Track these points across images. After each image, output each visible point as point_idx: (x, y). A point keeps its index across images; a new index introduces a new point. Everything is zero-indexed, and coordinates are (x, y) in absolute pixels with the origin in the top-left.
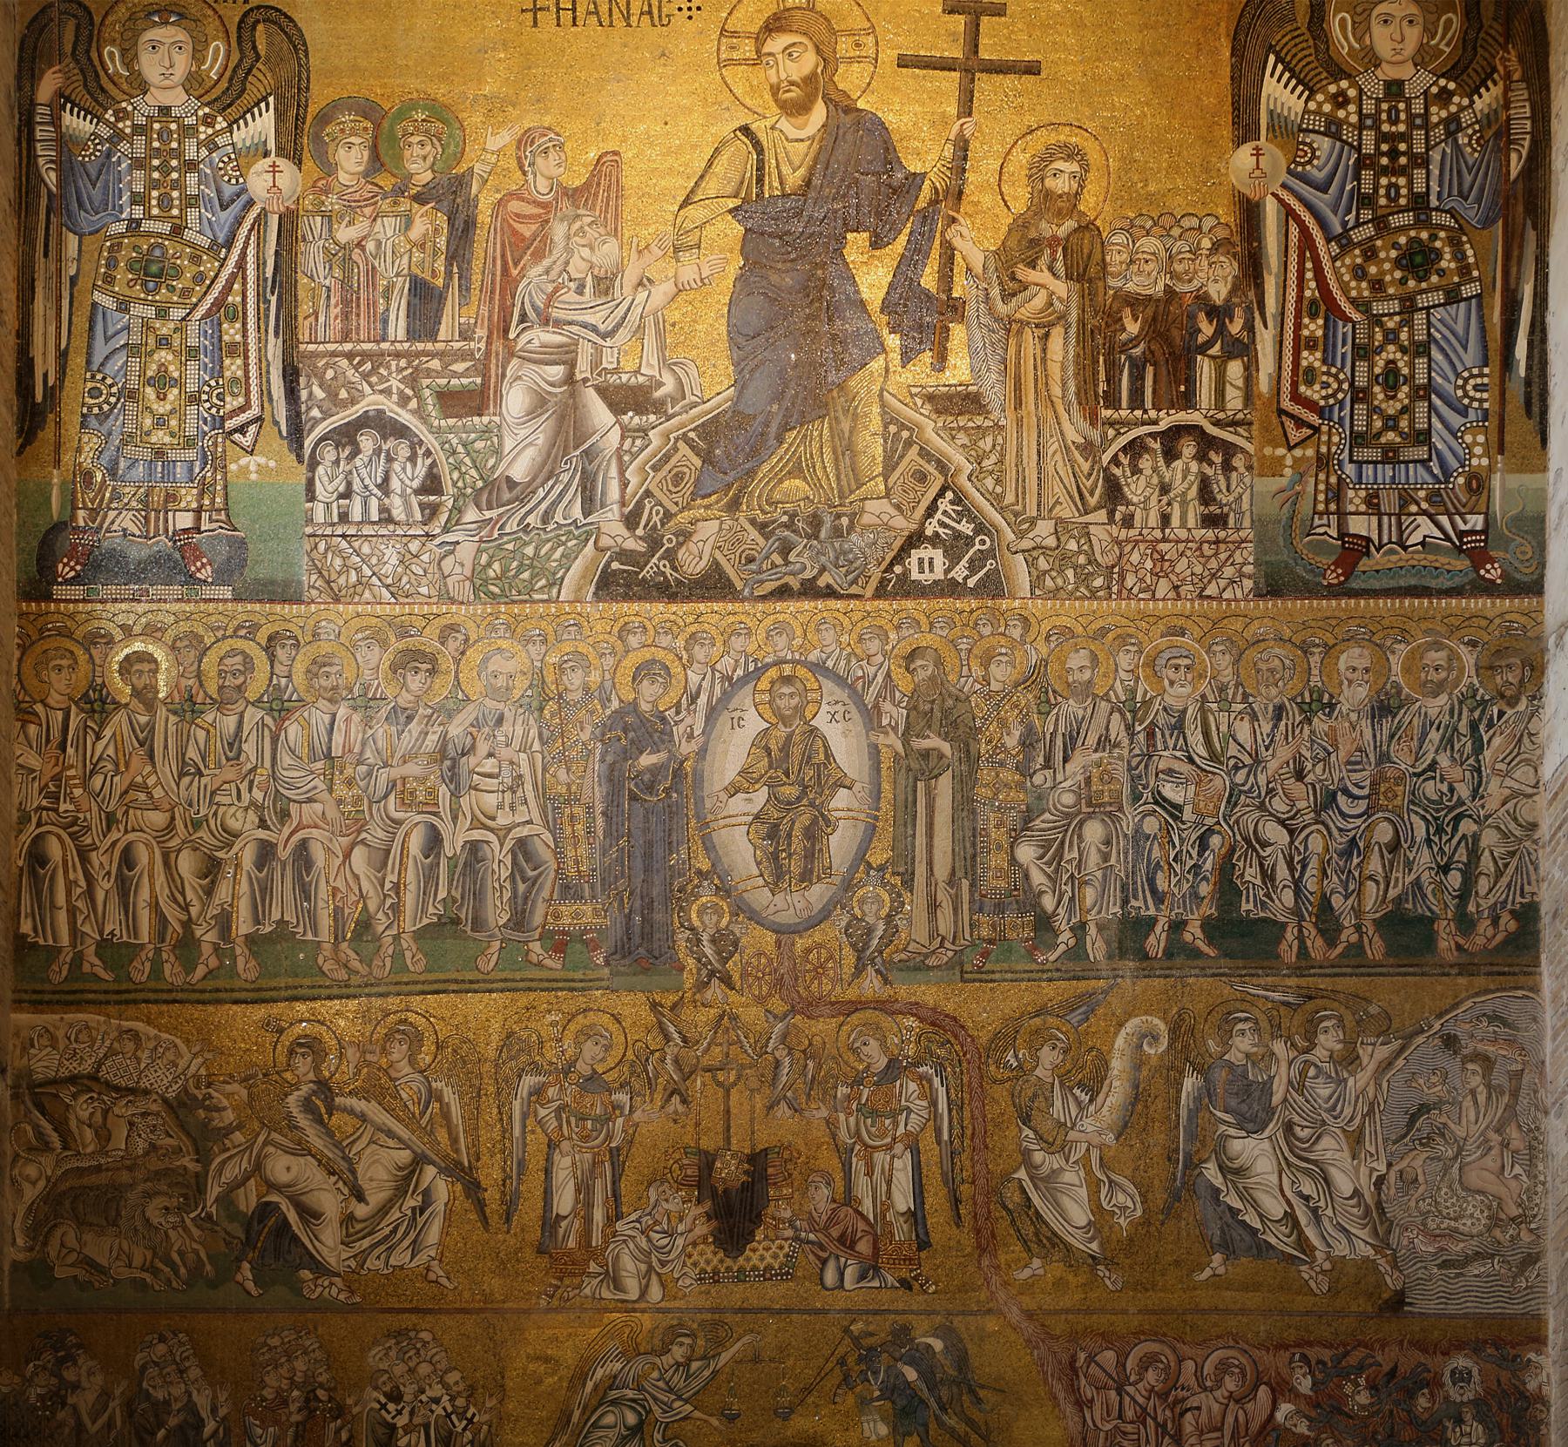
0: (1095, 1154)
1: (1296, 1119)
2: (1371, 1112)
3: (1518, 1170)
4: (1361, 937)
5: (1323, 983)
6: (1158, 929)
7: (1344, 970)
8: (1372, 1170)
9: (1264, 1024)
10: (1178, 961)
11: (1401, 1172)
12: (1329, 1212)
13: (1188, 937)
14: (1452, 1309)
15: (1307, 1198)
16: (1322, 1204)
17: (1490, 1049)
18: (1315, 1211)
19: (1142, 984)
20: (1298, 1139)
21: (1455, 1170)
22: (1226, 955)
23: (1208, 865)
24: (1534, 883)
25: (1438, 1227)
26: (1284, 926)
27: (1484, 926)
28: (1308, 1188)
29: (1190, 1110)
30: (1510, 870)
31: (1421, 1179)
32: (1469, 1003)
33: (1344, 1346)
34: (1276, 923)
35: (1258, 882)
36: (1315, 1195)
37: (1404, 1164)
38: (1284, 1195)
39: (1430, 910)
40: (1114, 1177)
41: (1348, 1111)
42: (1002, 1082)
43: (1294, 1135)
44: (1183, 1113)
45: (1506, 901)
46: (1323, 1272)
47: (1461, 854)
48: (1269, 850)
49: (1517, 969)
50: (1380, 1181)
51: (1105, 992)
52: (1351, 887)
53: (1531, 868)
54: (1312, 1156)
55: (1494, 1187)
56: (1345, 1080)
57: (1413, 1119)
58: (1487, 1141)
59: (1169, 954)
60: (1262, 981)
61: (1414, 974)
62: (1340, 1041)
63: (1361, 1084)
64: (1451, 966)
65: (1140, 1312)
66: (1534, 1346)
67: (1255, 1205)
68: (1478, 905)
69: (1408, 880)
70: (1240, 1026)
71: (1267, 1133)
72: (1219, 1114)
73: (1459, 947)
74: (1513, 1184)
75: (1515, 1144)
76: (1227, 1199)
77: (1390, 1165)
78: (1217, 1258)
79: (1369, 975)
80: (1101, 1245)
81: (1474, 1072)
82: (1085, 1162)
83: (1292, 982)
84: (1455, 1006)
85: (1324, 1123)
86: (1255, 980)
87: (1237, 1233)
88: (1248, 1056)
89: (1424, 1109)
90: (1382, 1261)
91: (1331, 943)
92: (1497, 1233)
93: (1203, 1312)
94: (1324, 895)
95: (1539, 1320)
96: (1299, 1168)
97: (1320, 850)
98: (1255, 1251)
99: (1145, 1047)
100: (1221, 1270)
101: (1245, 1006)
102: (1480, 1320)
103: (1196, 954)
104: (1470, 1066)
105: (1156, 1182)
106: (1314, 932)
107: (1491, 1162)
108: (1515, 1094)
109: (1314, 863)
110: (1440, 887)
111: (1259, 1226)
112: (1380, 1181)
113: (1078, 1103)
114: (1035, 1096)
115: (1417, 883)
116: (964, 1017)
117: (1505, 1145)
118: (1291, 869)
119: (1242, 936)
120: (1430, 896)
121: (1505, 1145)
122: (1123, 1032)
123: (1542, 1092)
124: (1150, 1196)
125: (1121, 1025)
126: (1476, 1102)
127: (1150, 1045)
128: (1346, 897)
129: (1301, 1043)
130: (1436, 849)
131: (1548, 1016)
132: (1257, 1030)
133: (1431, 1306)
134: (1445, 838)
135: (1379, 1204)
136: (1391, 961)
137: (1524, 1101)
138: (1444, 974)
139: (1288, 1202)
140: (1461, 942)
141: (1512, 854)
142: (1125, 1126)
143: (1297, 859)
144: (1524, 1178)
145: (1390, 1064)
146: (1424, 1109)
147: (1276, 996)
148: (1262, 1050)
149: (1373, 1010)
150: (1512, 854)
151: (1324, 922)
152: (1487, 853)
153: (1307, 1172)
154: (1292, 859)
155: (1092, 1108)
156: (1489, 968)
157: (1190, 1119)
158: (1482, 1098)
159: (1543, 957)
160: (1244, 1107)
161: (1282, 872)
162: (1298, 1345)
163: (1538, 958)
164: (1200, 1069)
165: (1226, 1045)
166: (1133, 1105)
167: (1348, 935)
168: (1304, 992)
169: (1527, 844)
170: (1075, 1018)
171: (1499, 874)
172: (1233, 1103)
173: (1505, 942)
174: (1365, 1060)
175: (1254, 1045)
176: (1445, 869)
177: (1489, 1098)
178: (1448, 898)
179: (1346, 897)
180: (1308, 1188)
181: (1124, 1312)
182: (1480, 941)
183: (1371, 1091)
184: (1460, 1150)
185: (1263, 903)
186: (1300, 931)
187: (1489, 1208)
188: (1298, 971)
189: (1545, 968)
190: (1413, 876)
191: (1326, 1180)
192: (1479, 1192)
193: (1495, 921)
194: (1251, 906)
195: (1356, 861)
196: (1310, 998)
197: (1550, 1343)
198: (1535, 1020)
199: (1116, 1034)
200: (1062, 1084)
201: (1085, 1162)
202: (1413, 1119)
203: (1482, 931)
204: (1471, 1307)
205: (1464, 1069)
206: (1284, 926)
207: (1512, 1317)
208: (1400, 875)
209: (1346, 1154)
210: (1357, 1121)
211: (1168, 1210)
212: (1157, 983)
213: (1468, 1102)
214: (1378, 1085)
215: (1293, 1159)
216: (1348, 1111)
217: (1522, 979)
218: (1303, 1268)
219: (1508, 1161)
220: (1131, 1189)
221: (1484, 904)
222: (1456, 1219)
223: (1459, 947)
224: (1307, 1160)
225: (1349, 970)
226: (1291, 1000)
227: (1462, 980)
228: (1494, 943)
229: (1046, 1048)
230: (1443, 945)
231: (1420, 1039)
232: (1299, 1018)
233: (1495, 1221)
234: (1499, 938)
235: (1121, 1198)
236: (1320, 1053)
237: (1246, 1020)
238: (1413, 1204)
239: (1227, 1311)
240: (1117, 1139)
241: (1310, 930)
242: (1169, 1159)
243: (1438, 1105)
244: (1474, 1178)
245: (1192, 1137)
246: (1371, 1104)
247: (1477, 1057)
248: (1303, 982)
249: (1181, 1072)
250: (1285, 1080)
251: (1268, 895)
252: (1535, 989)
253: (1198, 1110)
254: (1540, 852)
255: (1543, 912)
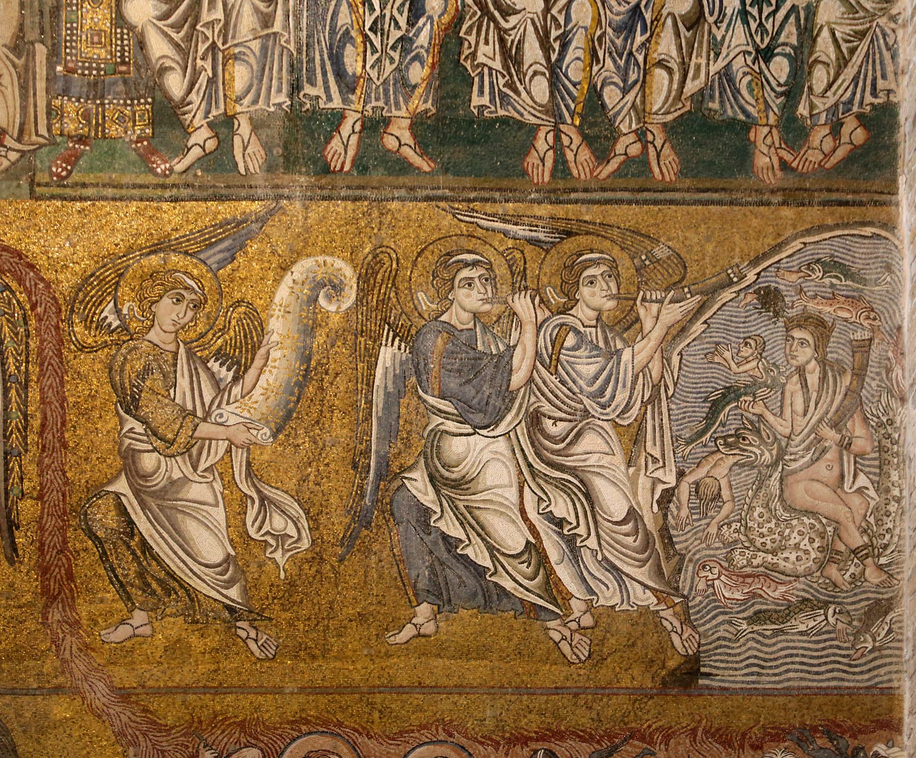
0: (239, 458)
1: (547, 408)
2: (654, 399)
3: (862, 480)
4: (645, 148)
5: (589, 214)
6: (346, 129)
7: (619, 195)
8: (656, 481)
9: (501, 270)
10: (377, 176)
11: (697, 484)
12: (592, 542)
13: (390, 143)
14: (767, 682)
15: (560, 523)
16: (582, 530)
17: (827, 310)
18: (571, 541)
19: (319, 209)
20: (548, 437)
21: (774, 482)
22: (446, 171)
23: (423, 39)
24: (891, 76)
25: (749, 564)
26: (534, 129)
27: (820, 136)
28: (561, 507)
29: (387, 395)
30: (858, 58)
31: (725, 494)
32: (797, 245)
33: (610, 738)
34: (521, 125)
35: (497, 65)
36: (572, 519)
37: (701, 473)
38: (525, 518)
39: (744, 111)
40: (268, 491)
41: (622, 397)
42: (92, 349)
43: (543, 431)
44: (378, 398)
45: (851, 102)
46: (581, 629)
47: (790, 35)
48: (513, 20)
49: (864, 198)
50: (667, 497)
51: (262, 220)
52: (633, 77)
53: (887, 55)
54: (569, 462)
55: (828, 505)
56: (618, 353)
57: (715, 408)
58: (819, 440)
59: (361, 165)
60: (499, 209)
61: (720, 203)
62: (611, 297)
63: (641, 358)
64: (773, 192)
65: (302, 690)
66: (885, 733)
67: (483, 533)
68: (812, 106)
69: (713, 69)
70: (465, 273)
71: (502, 428)
72: (431, 400)
73: (784, 165)
74: (856, 501)
75: (860, 444)
76: (442, 525)
77: (681, 475)
78: (424, 610)
79: (656, 202)
80: (245, 591)
81: (803, 342)
82: (223, 470)
83: (543, 210)
84: (777, 248)
85: (586, 413)
86: (489, 208)
87: (454, 574)
88: (476, 316)
89: (731, 394)
90: (667, 614)
91: (602, 155)
92: (833, 571)
93: (400, 690)
94: (592, 87)
95: (890, 694)
96: (547, 479)
97: (588, 22)
98: (480, 599)
99: (322, 301)
100: (429, 628)
101: (472, 244)
102: (805, 696)
103: (403, 167)
104: (797, 334)
105: (334, 500)
106: (577, 140)
107: (825, 470)
108: (860, 374)
109: (578, 41)
110: (760, 80)
111: (488, 563)
112: (667, 497)
113: (216, 382)
114: (147, 370)
115: (726, 74)
116: (33, 248)
117: (845, 445)
118: (546, 46)
119: (473, 143)
120: (744, 92)
121: (845, 445)
122: (288, 279)
123: (898, 371)
124: (323, 519)
125: (284, 268)
126: (804, 385)
127: (329, 298)
128: (625, 91)
129: (556, 299)
130: (754, 26)
131: (906, 263)
132: (490, 279)
133: (737, 678)
134: (766, 10)
135: (664, 531)
136: (688, 183)
137: (872, 384)
138: (762, 203)
139: (532, 529)
140: (788, 157)
141: (861, 35)
142: (288, 416)
143: (554, 34)
144: (872, 492)
145: (683, 330)
146: (731, 394)
147: (521, 231)
148: (497, 309)
149: (660, 252)
150: (861, 35)
151: (592, 125)
152: (825, 33)
153: (562, 486)
154: (547, 33)
155: (236, 390)
156: (825, 196)
157: (387, 406)
158: (813, 379)
159: (901, 180)
160: (470, 391)
161: (532, 52)
162: (541, 738)
163: (894, 181)
164: (404, 335)
165: (445, 298)
166: (301, 386)
167: (627, 145)
168: (562, 225)
169: (882, 21)
170: (214, 256)
171: (843, 62)
172: (453, 384)
173: (849, 160)
174: (648, 324)
175: (485, 301)
176: (767, 54)
177: (823, 378)
178: (769, 95)
179: (625, 91)
180: (561, 507)
181: (278, 690)
182: (814, 157)
183: (655, 368)
184: (782, 453)
185: (503, 96)
186: (557, 138)
187: (822, 535)
188: (552, 195)
189: (904, 195)
190: (721, 64)
191: (588, 496)
192: (808, 513)
193: (836, 129)
194: (485, 100)
195: (639, 39)
196: (569, 234)
197: (906, 730)
198: (888, 268)
199: (277, 281)
200: (190, 354)
201: (223, 470)
202: (715, 408)
203: (816, 143)
204: (794, 679)
205: (788, 338)
206: (534, 129)
207: (852, 692)
208: (703, 61)
209: (619, 459)
210: (635, 411)
211: (350, 541)
212: (342, 208)
213: (793, 385)
214: (666, 360)
215: (539, 466)
216: (622, 397)
217: (871, 212)
218: (551, 624)
219: (849, 469)
220: (295, 509)
221: (821, 105)
222: (774, 552)
223: (784, 165)
224: (561, 468)
225: (626, 195)
226: (541, 236)
227: (788, 212)
228: (834, 160)
229: (166, 301)
230: (762, 161)
231: (727, 295)
232: (553, 261)
233: (829, 555)
234: (841, 153)
235: (278, 522)
236: (583, 313)
237: (475, 264)
238: (713, 530)
239: (436, 689)
240: (275, 435)
241: (572, 136)
242: (355, 466)
243: (751, 388)
244: (800, 493)
245: (390, 432)
246: (656, 387)
247: (807, 320)
248: (560, 211)
249: (377, 339)
250: (530, 351)
251: (511, 85)
252: (890, 225)
253: (400, 394)
254: (900, 33)
255: (902, 117)
